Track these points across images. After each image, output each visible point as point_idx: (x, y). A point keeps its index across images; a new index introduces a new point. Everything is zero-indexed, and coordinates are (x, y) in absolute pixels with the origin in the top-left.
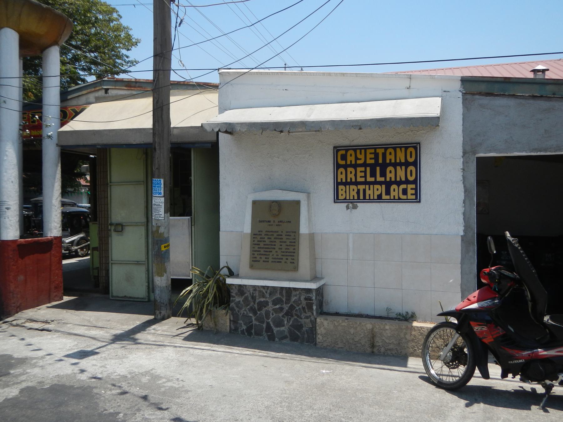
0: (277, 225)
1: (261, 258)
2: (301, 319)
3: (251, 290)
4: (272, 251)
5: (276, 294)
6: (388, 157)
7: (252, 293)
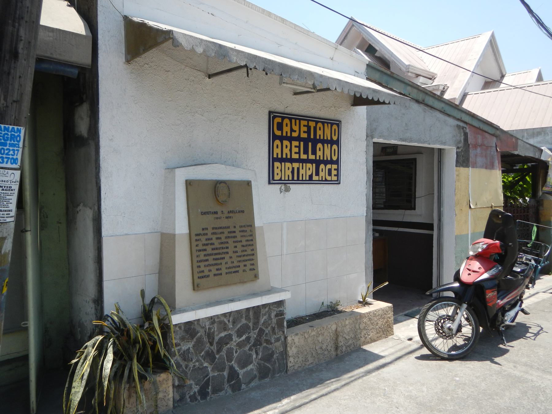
0: (227, 218)
1: (210, 271)
2: (271, 343)
3: (207, 324)
4: (224, 258)
5: (242, 320)
6: (319, 133)
7: (209, 329)
